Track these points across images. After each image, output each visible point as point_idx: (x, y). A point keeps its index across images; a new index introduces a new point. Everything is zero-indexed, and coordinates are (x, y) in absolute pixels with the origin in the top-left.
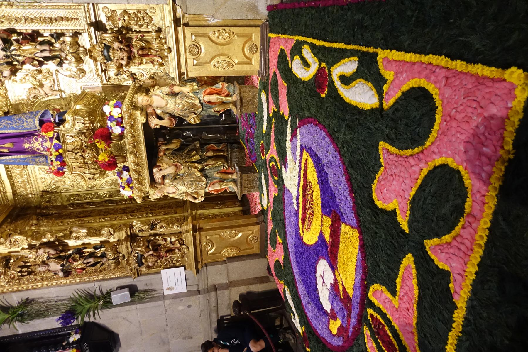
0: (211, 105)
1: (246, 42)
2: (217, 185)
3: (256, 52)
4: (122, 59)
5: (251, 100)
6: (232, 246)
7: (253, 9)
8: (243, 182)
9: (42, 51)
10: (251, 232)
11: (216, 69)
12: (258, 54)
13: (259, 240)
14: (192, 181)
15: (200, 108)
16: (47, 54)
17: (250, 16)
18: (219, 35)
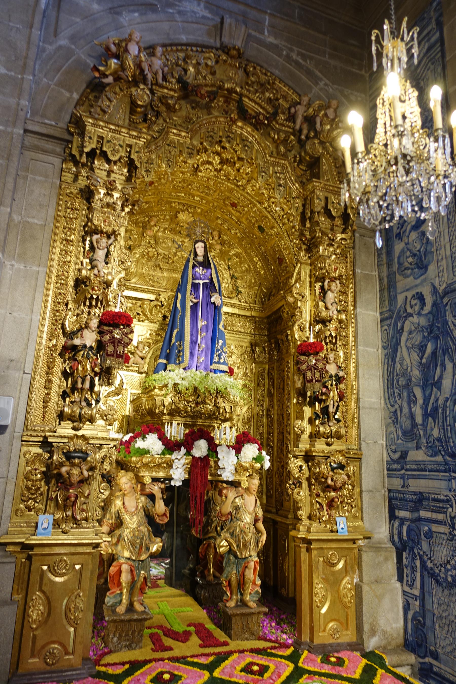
0: (241, 570)
1: (341, 623)
2: (129, 577)
3: (334, 638)
4: (332, 480)
5: (249, 628)
6: (49, 614)
7: (373, 629)
8: (133, 624)
9: (334, 406)
10: (70, 649)
11: (314, 585)
12: (331, 641)
13: (48, 668)
14: (142, 538)
15: (241, 554)
16: (331, 410)
17: (366, 628)
18: (349, 589)
